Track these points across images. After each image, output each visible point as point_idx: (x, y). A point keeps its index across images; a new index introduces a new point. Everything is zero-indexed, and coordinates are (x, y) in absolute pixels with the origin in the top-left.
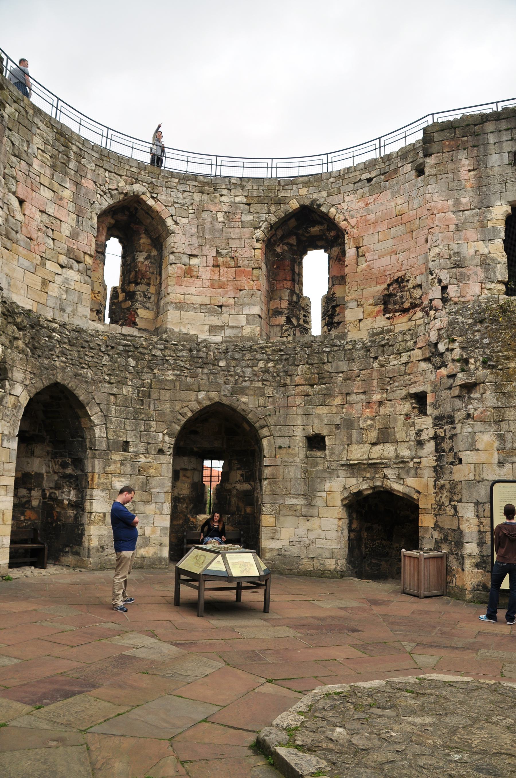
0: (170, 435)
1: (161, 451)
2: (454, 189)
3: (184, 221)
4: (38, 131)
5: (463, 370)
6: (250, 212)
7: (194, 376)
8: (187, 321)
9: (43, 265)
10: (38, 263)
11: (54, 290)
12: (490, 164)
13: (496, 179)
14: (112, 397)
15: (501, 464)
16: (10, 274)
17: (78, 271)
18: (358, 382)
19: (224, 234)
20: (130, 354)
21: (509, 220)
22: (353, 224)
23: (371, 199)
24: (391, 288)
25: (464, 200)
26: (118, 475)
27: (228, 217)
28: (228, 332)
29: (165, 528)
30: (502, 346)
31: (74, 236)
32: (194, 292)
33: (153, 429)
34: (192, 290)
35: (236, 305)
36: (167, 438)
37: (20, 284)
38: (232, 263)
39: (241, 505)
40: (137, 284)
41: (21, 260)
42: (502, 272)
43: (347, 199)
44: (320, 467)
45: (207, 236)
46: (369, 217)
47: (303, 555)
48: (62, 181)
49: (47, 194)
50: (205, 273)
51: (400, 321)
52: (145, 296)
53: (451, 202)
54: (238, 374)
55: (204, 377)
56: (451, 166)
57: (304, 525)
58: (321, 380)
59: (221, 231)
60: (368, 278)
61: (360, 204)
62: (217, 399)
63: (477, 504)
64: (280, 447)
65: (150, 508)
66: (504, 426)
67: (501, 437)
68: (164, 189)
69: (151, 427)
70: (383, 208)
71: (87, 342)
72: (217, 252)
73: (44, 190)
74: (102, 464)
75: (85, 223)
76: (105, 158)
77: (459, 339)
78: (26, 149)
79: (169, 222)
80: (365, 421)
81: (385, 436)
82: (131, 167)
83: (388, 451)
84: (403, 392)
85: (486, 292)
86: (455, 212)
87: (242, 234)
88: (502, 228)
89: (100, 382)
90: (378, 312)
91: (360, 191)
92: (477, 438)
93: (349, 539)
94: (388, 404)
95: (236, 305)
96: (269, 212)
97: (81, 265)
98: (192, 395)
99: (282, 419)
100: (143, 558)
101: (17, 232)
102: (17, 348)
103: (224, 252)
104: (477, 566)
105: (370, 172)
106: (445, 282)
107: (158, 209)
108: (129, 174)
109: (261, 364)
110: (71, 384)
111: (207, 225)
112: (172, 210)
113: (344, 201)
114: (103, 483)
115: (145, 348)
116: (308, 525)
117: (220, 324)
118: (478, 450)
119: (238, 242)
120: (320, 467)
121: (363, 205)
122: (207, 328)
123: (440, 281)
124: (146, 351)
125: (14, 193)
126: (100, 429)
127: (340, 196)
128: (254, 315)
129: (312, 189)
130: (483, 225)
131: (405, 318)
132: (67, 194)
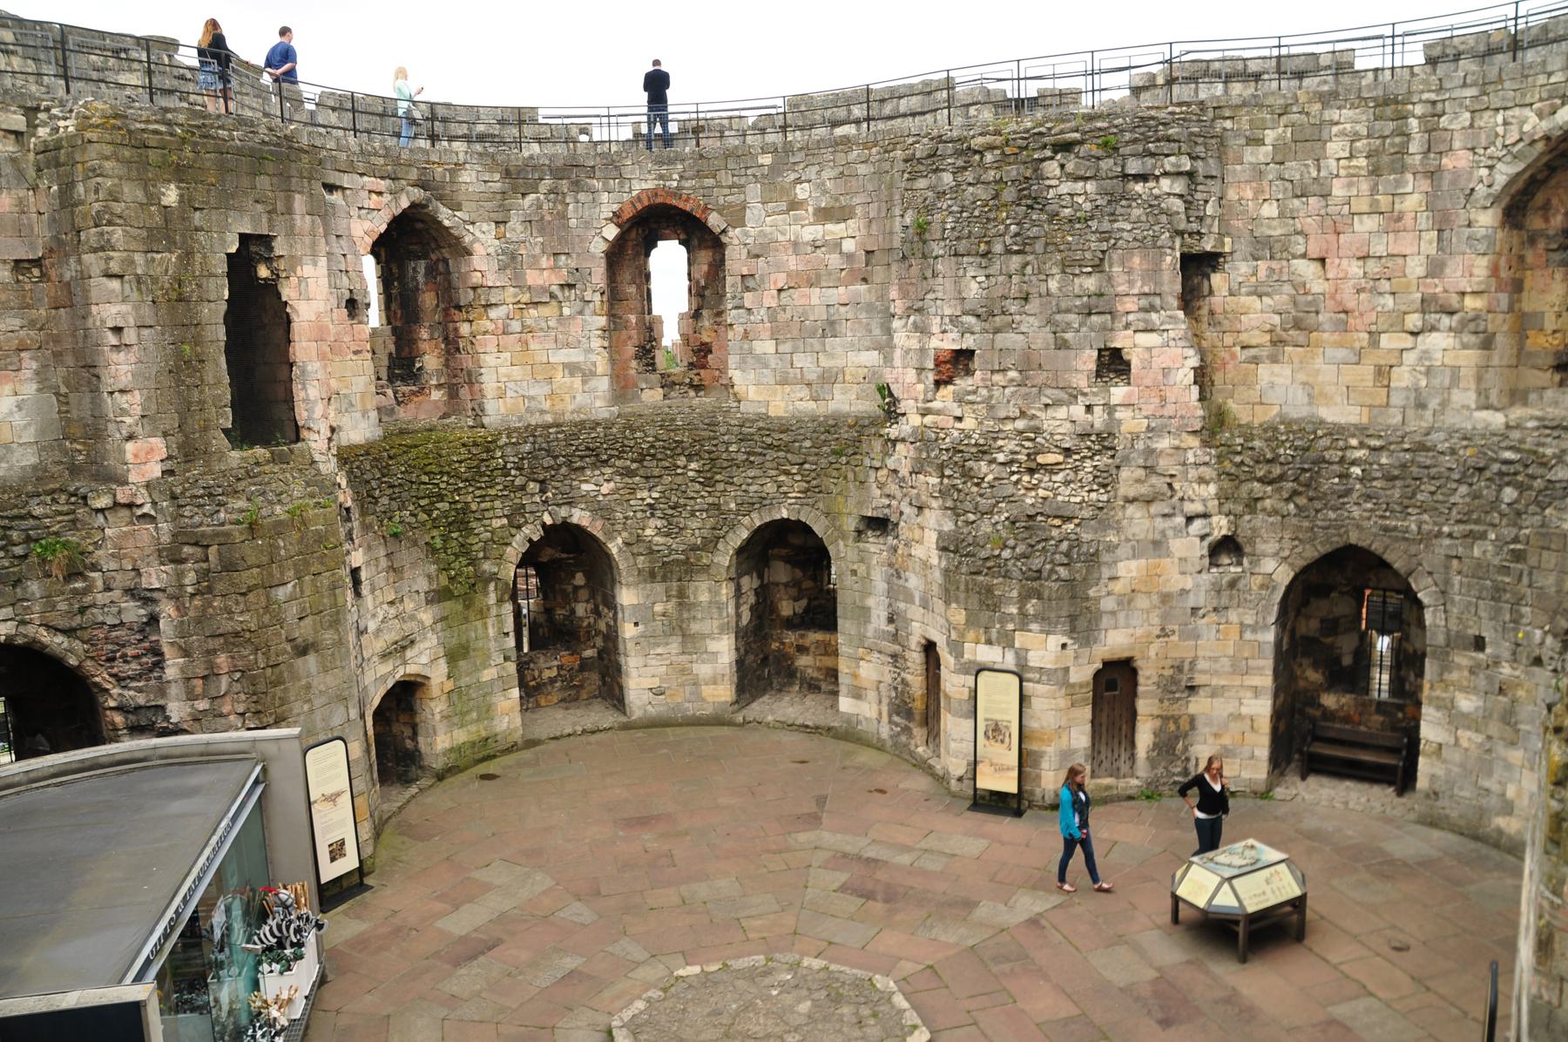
1: (1538, 661)
4: (1335, 129)
9: (1374, 343)
10: (1365, 344)
11: (1402, 378)
14: (1455, 562)
16: (1311, 380)
17: (1450, 329)
20: (1507, 479)
26: (1466, 690)
31: (1435, 268)
33: (1524, 621)
36: (1549, 640)
37: (1330, 390)
41: (1329, 352)
48: (1397, 187)
49: (1370, 223)
65: (1516, 756)
69: (1522, 616)
71: (1427, 467)
73: (1361, 222)
74: (1436, 668)
75: (1457, 238)
78: (1314, 174)
89: (1436, 537)
97: (1456, 317)
101: (1317, 313)
102: (1264, 510)
110: (1376, 547)
114: (1438, 698)
115: (1544, 465)
124: (1540, 471)
125: (1304, 256)
126: (1434, 613)
132: (1412, 202)
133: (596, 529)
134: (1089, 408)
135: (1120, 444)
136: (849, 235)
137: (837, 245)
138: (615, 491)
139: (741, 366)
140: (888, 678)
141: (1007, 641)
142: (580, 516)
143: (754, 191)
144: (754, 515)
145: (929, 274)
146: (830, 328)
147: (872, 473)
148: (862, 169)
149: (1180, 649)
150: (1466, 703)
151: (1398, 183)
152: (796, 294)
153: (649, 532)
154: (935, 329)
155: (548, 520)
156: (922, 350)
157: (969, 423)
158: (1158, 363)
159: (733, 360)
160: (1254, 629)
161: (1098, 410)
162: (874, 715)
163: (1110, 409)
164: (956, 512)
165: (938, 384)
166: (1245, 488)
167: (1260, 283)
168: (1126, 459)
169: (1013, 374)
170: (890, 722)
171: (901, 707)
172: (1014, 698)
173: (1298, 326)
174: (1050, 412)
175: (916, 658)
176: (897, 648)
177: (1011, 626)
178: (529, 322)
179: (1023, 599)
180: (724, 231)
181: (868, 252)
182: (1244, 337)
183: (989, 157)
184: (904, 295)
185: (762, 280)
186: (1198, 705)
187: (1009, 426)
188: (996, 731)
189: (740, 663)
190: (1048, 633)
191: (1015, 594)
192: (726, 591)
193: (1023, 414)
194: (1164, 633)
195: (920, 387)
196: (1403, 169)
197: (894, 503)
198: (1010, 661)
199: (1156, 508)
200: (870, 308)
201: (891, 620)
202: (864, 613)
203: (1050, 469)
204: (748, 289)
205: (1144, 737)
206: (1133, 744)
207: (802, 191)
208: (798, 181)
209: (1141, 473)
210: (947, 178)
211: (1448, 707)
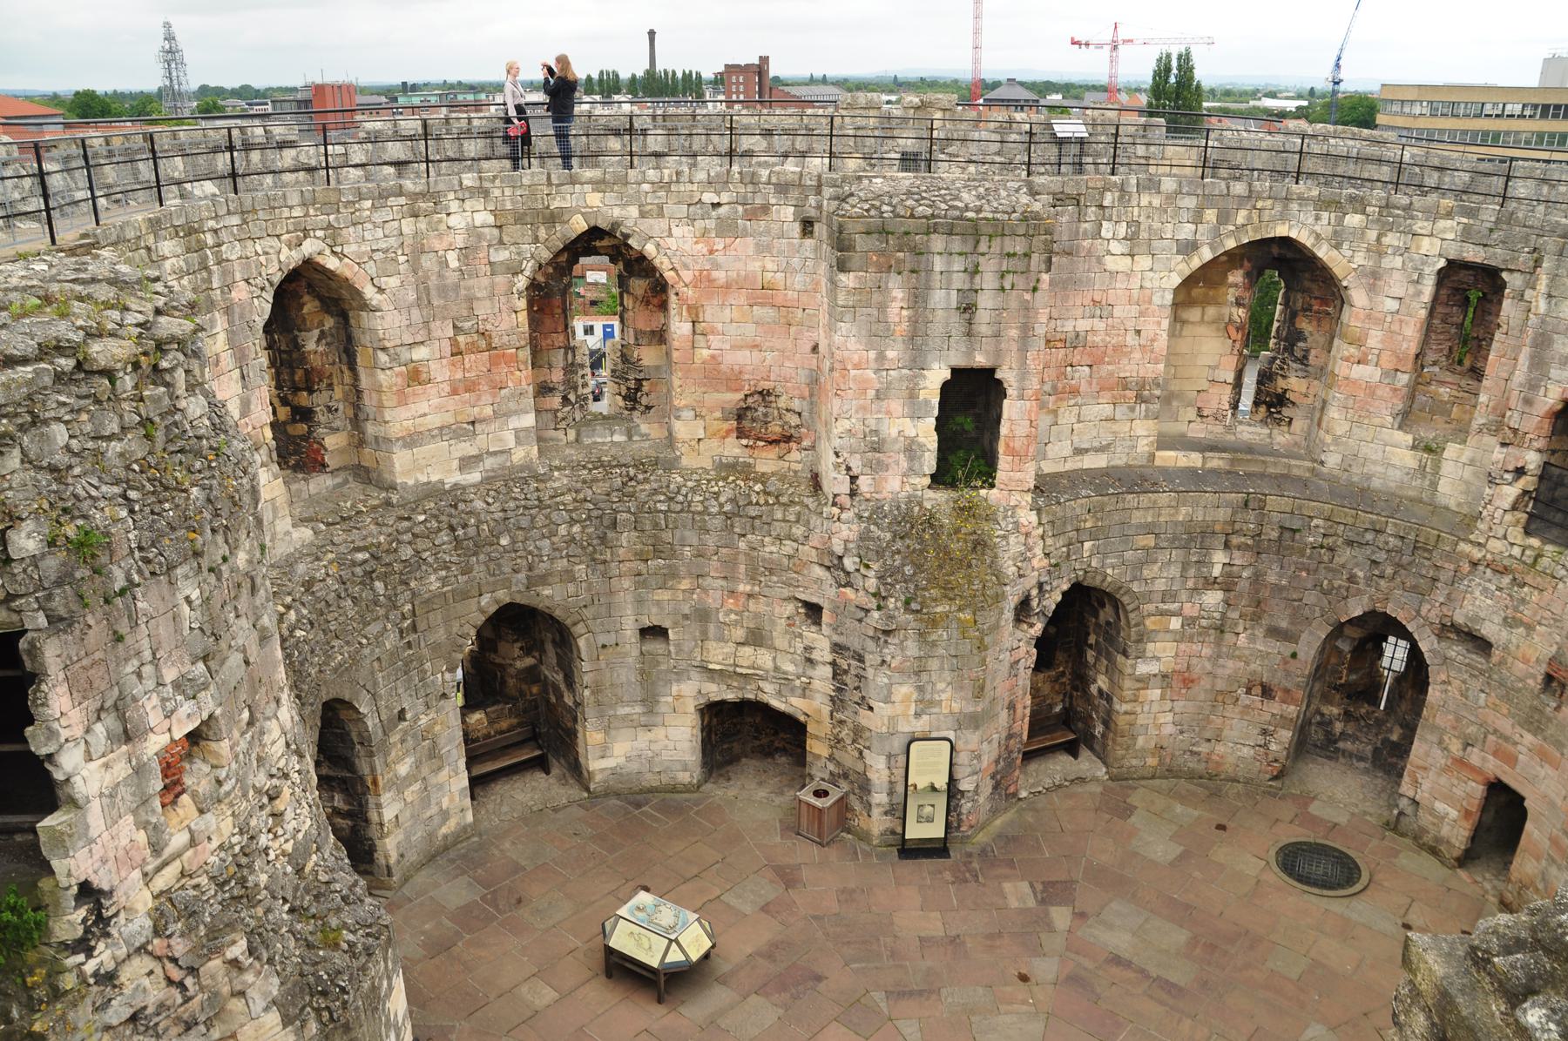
1: (444, 696)
2: (877, 334)
3: (392, 282)
5: (879, 608)
6: (501, 242)
7: (466, 571)
8: (423, 462)
12: (931, 305)
13: (937, 329)
15: (917, 715)
18: (714, 563)
19: (463, 292)
21: (946, 388)
22: (687, 280)
23: (719, 244)
24: (750, 400)
25: (891, 354)
27: (466, 257)
28: (490, 463)
30: (929, 581)
32: (427, 408)
34: (423, 407)
35: (496, 415)
38: (483, 344)
39: (524, 687)
40: (311, 391)
42: (930, 463)
43: (676, 231)
44: (663, 667)
45: (435, 303)
46: (715, 274)
47: (645, 769)
50: (441, 372)
51: (764, 455)
52: (329, 409)
53: (872, 354)
54: (530, 553)
55: (483, 568)
56: (876, 297)
57: (644, 738)
58: (658, 553)
59: (457, 287)
60: (715, 376)
61: (700, 246)
62: (508, 600)
63: (889, 756)
64: (604, 646)
66: (924, 676)
67: (920, 689)
68: (351, 229)
70: (740, 265)
72: (455, 327)
76: (250, 217)
77: (875, 566)
79: (369, 292)
80: (727, 615)
81: (756, 638)
82: (291, 208)
83: (765, 658)
84: (786, 593)
85: (908, 488)
86: (877, 371)
87: (493, 286)
88: (936, 400)
90: (728, 432)
91: (699, 224)
94: (762, 599)
95: (496, 415)
96: (536, 240)
99: (603, 610)
100: (445, 837)
103: (467, 325)
104: (886, 813)
105: (718, 193)
106: (855, 471)
107: (348, 274)
108: (291, 228)
109: (563, 530)
111: (433, 282)
112: (371, 268)
113: (670, 235)
115: (388, 551)
116: (650, 736)
117: (474, 452)
119: (488, 303)
120: (663, 667)
121: (705, 251)
122: (455, 464)
123: (849, 469)
127: (663, 223)
128: (526, 429)
129: (611, 197)
130: (912, 395)
131: (773, 452)
145: (123, 628)
150: (403, 769)
154: (155, 718)
156: (139, 771)
184: (80, 689)
210: (59, 433)
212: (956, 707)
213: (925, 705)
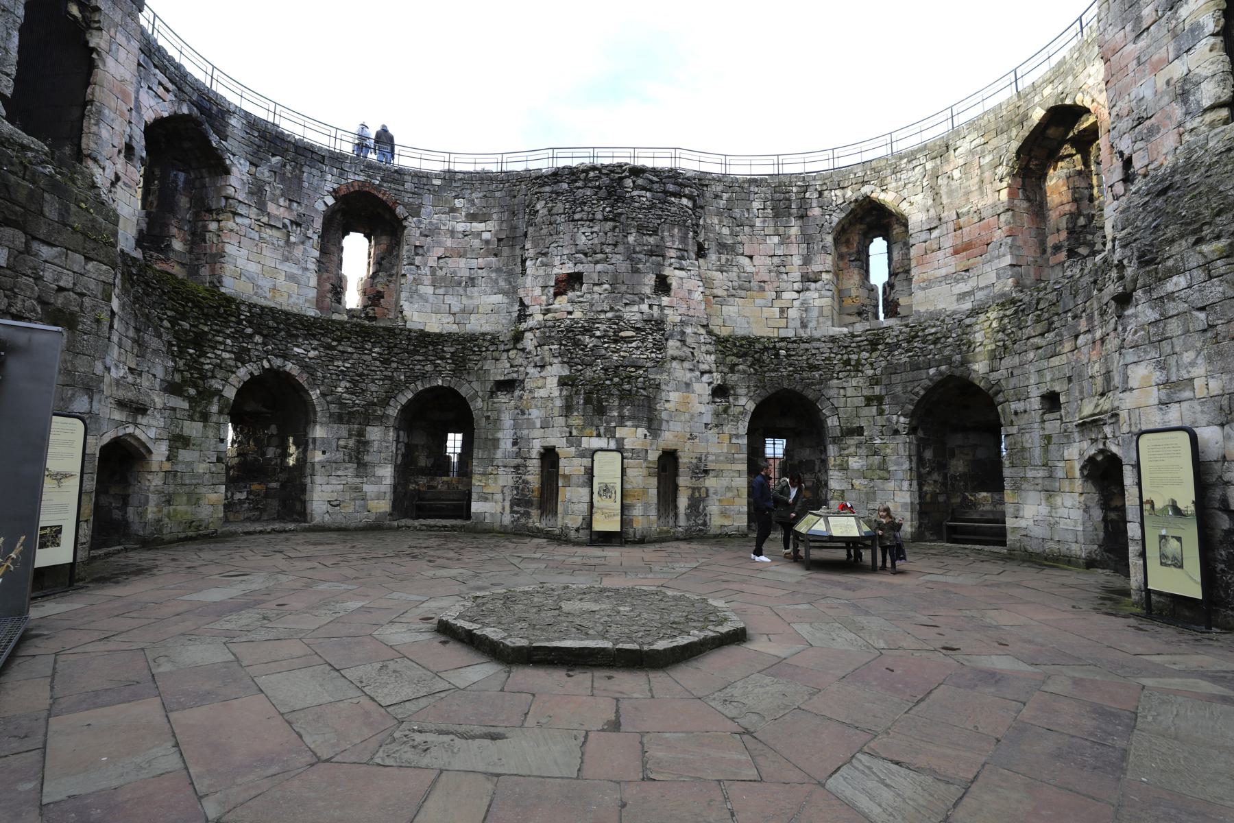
0: (905, 416)
11: (793, 313)
15: (1164, 404)
29: (906, 504)
31: (807, 260)
36: (902, 419)
49: (776, 239)
65: (891, 485)
92: (1129, 372)
93: (1105, 519)
98: (923, 373)
111: (943, 191)
118: (1131, 389)
122: (955, 298)
132: (794, 231)
133: (303, 379)
134: (651, 306)
135: (668, 328)
136: (487, 230)
137: (479, 234)
138: (319, 357)
139: (410, 299)
140: (510, 482)
141: (610, 433)
142: (290, 367)
143: (428, 199)
144: (419, 383)
146: (472, 281)
147: (505, 355)
148: (498, 194)
149: (701, 448)
151: (787, 222)
152: (450, 261)
153: (339, 390)
155: (266, 365)
157: (577, 315)
158: (686, 286)
159: (403, 295)
160: (738, 436)
161: (655, 308)
162: (499, 509)
163: (662, 308)
164: (570, 363)
165: (556, 295)
166: (729, 359)
167: (722, 265)
168: (671, 335)
169: (606, 286)
170: (512, 512)
171: (520, 501)
172: (608, 474)
173: (745, 287)
174: (628, 308)
175: (534, 464)
176: (519, 461)
177: (613, 424)
178: (264, 235)
179: (621, 407)
180: (406, 219)
181: (500, 240)
182: (715, 291)
183: (592, 174)
184: (535, 246)
185: (428, 250)
186: (710, 482)
187: (602, 316)
188: (606, 490)
189: (395, 487)
190: (637, 427)
191: (616, 403)
192: (391, 434)
193: (612, 309)
194: (692, 437)
195: (544, 298)
196: (790, 215)
197: (522, 369)
198: (613, 445)
199: (687, 365)
200: (498, 270)
201: (515, 443)
202: (495, 443)
203: (627, 340)
204: (417, 254)
205: (683, 502)
206: (676, 507)
207: (459, 203)
208: (457, 197)
209: (678, 344)
210: (565, 186)
211: (844, 468)
212: (1215, 386)
213: (1173, 389)
